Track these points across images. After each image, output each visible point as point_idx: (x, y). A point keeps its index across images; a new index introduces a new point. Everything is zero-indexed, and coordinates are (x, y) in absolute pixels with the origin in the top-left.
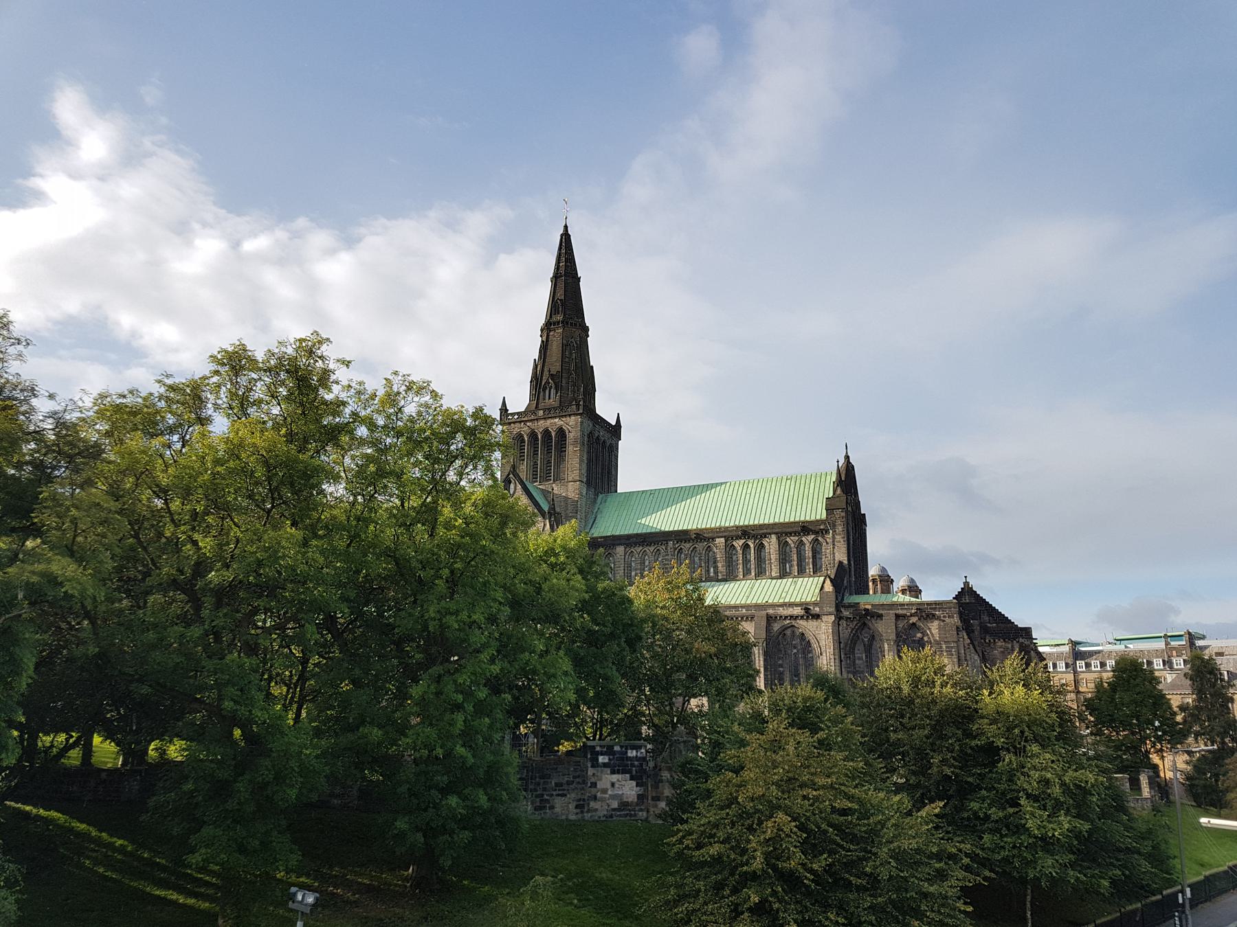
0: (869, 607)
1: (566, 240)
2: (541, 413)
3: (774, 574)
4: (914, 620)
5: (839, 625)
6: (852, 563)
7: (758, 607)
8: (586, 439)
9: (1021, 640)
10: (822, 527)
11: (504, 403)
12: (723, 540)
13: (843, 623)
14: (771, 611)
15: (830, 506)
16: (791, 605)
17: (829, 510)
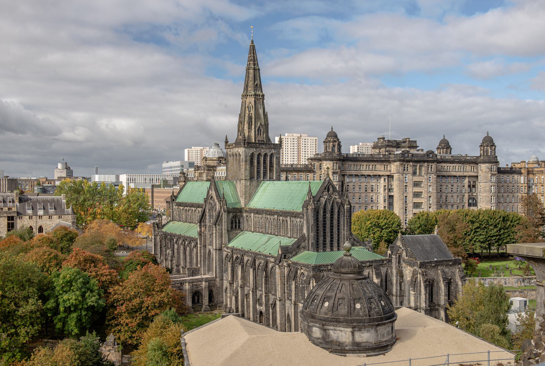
0: (291, 263)
1: (253, 49)
2: (234, 145)
3: (289, 236)
4: (302, 271)
5: (284, 269)
6: (312, 235)
7: (266, 256)
8: (248, 158)
9: (416, 268)
10: (301, 216)
11: (226, 139)
12: (276, 216)
13: (285, 268)
14: (268, 258)
15: (306, 205)
16: (272, 257)
17: (303, 207)
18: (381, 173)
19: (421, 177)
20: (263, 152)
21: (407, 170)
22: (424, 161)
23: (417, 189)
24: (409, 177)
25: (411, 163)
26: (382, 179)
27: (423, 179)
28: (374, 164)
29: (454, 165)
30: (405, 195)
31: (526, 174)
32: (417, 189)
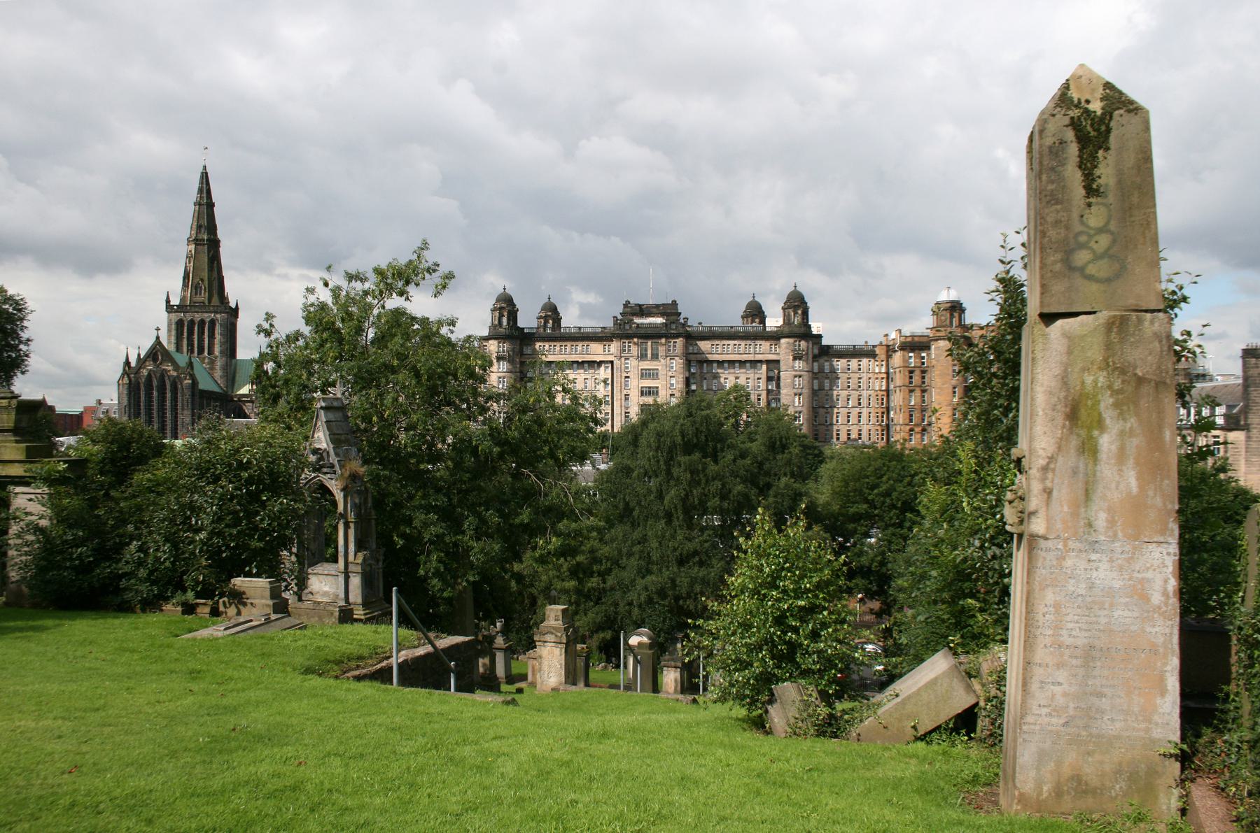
1: (205, 178)
18: (598, 359)
19: (655, 363)
20: (198, 317)
21: (629, 351)
22: (659, 336)
23: (648, 383)
24: (633, 363)
25: (636, 340)
26: (602, 368)
27: (659, 365)
28: (586, 343)
29: (736, 342)
30: (625, 392)
31: (883, 357)
32: (648, 383)
